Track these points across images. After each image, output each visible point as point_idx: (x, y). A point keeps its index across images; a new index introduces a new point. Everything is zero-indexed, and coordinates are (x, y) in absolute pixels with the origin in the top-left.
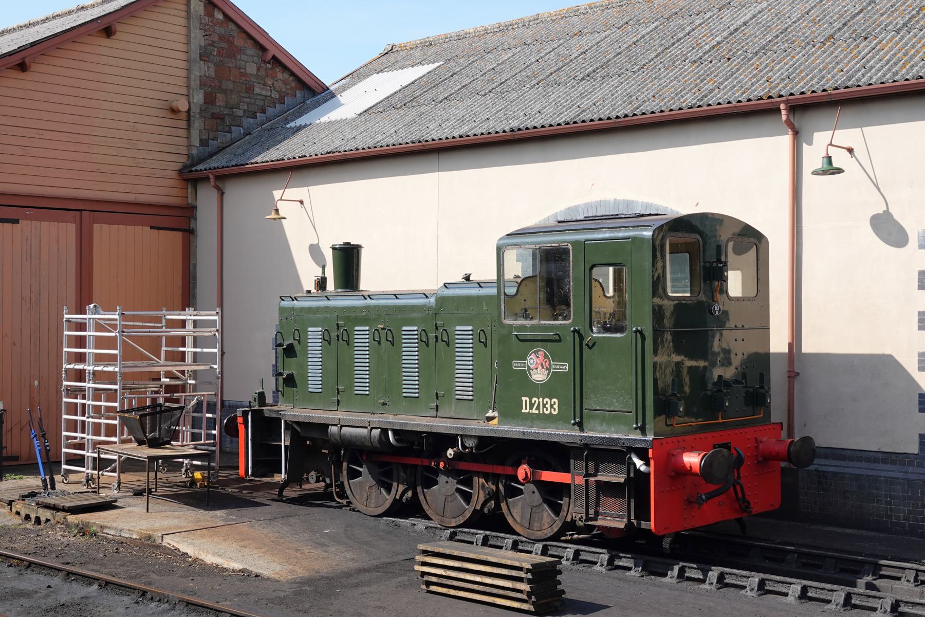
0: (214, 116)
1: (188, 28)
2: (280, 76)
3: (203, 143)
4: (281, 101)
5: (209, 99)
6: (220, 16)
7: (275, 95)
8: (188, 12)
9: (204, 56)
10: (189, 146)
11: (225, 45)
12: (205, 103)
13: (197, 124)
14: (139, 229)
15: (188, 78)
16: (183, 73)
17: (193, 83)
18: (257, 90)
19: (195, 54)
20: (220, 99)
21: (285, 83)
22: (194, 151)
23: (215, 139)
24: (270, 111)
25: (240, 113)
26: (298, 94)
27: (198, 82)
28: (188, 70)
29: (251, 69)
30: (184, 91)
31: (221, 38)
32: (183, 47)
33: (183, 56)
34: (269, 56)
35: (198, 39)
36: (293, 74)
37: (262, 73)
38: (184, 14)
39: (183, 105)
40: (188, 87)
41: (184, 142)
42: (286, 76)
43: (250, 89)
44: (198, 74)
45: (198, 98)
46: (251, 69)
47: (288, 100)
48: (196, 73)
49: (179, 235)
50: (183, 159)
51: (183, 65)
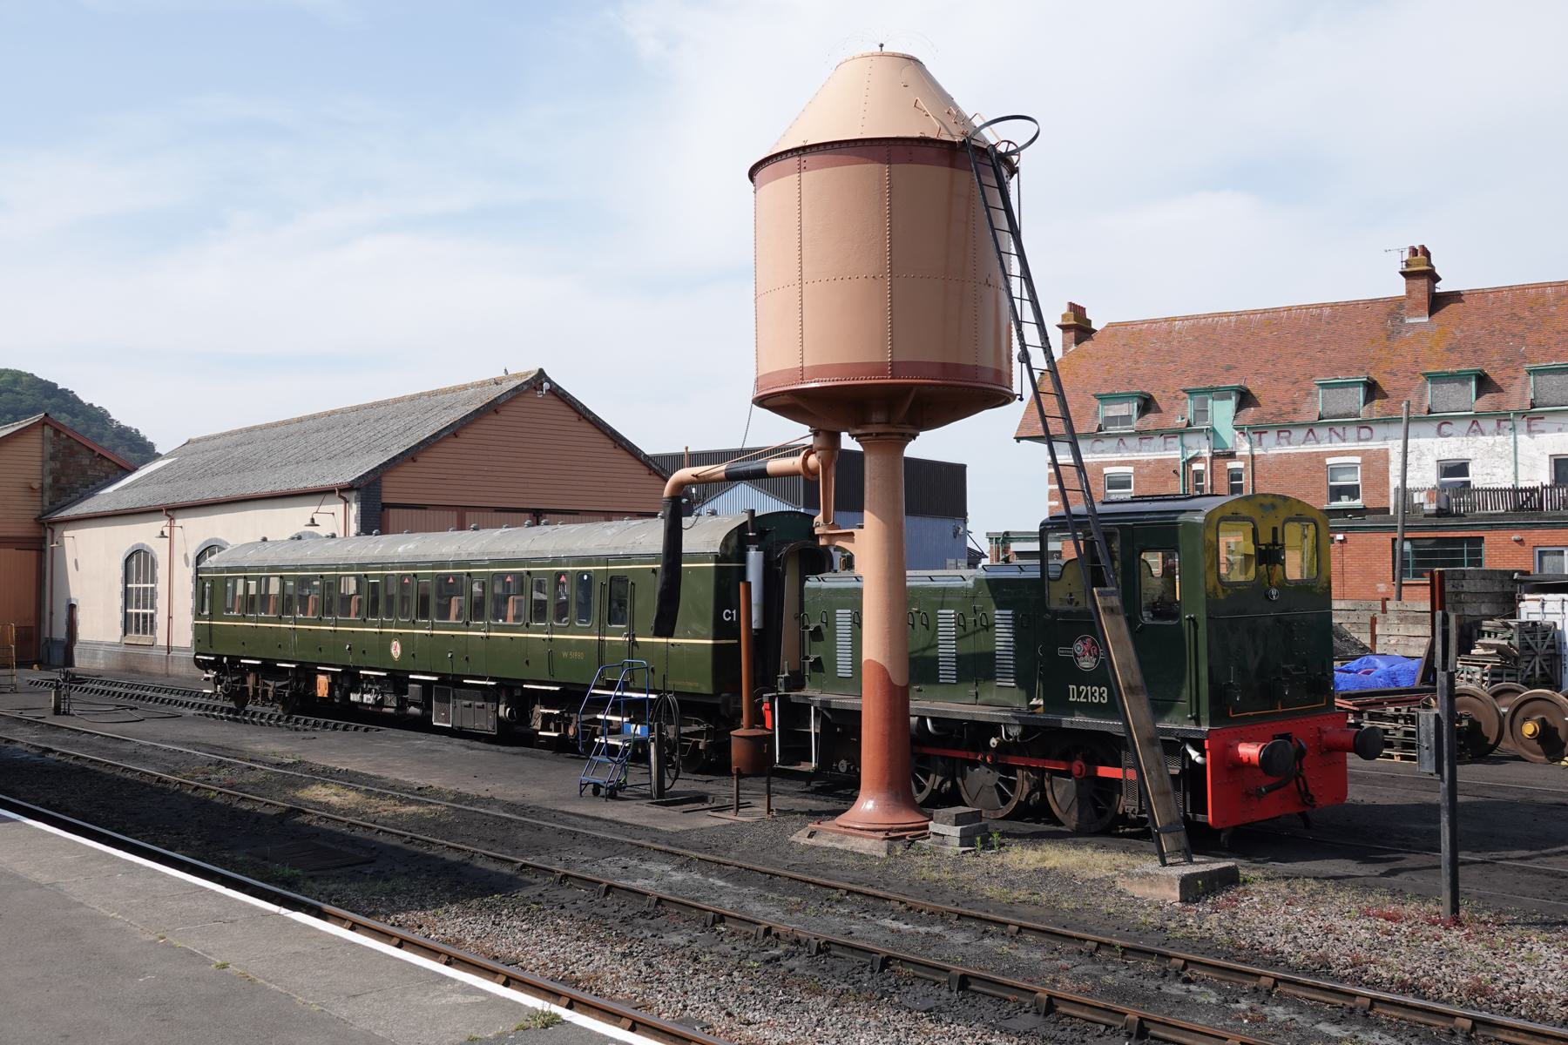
0: (59, 489)
1: (43, 444)
2: (106, 463)
3: (51, 503)
4: (107, 477)
5: (56, 480)
6: (64, 436)
7: (102, 474)
8: (43, 435)
9: (53, 458)
10: (43, 506)
11: (67, 451)
12: (53, 482)
13: (48, 494)
14: (9, 551)
15: (42, 470)
16: (40, 468)
17: (45, 473)
18: (89, 473)
19: (47, 457)
20: (63, 480)
21: (110, 467)
22: (46, 508)
23: (60, 501)
24: (98, 483)
25: (78, 486)
26: (119, 473)
27: (48, 471)
28: (43, 466)
29: (86, 462)
30: (40, 477)
31: (65, 447)
32: (40, 455)
33: (40, 459)
34: (96, 454)
35: (49, 449)
36: (114, 462)
37: (93, 463)
38: (40, 437)
39: (36, 485)
40: (43, 475)
41: (38, 503)
42: (110, 463)
43: (84, 473)
44: (48, 467)
45: (49, 480)
46: (86, 462)
47: (111, 476)
48: (48, 467)
49: (34, 553)
50: (39, 513)
51: (40, 463)
